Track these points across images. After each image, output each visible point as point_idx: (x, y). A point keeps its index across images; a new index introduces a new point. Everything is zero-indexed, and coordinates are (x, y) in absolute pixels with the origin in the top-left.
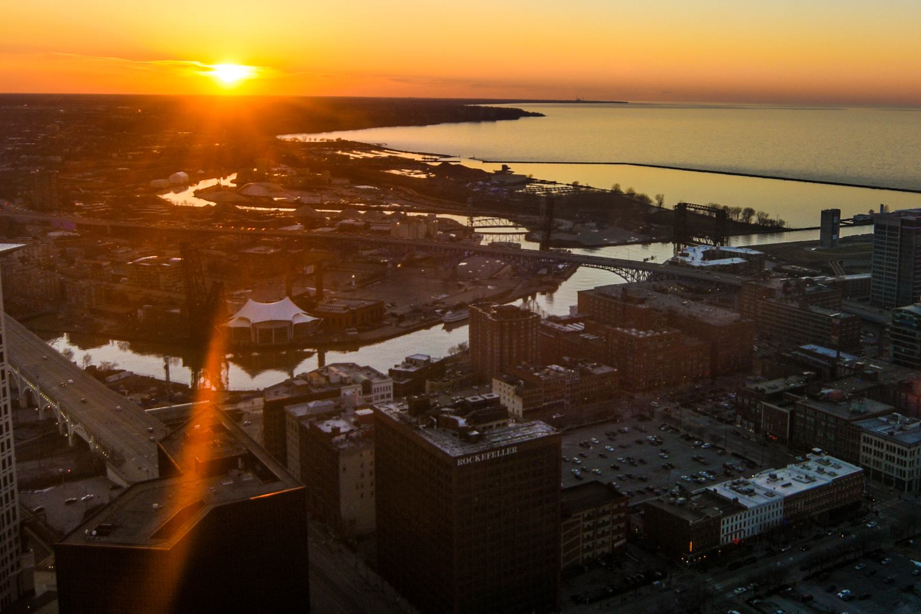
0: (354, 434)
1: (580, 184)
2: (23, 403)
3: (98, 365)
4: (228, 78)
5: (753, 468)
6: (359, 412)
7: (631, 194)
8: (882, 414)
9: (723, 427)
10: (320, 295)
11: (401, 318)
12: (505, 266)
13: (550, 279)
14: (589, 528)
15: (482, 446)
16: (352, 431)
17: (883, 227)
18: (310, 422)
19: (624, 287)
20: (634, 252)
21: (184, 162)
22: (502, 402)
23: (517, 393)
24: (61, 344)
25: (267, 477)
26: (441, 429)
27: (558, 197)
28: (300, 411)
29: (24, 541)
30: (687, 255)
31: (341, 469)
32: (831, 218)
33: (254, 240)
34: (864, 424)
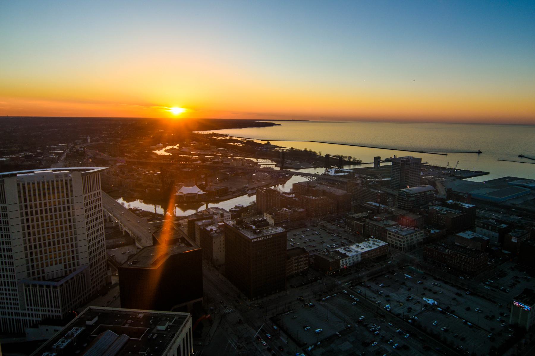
2: (108, 220)
4: (176, 112)
5: (351, 243)
6: (219, 224)
7: (311, 151)
8: (395, 225)
10: (206, 185)
11: (234, 192)
13: (283, 179)
14: (296, 263)
17: (395, 163)
19: (308, 183)
20: (311, 171)
21: (160, 140)
23: (272, 218)
24: (120, 201)
25: (189, 245)
27: (286, 152)
29: (108, 266)
32: (377, 160)
33: (185, 166)
34: (388, 228)
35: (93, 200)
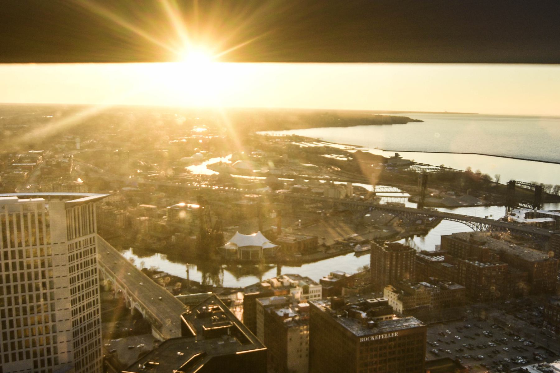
0: (297, 318)
1: (445, 166)
3: (149, 268)
6: (302, 305)
9: (534, 328)
10: (279, 232)
11: (328, 248)
12: (394, 218)
13: (423, 227)
15: (376, 330)
16: (296, 316)
18: (271, 309)
19: (471, 235)
20: (479, 212)
22: (390, 303)
23: (399, 299)
24: (128, 255)
26: (350, 318)
27: (431, 174)
28: (265, 302)
30: (514, 215)
31: (288, 339)
35: (82, 250)
